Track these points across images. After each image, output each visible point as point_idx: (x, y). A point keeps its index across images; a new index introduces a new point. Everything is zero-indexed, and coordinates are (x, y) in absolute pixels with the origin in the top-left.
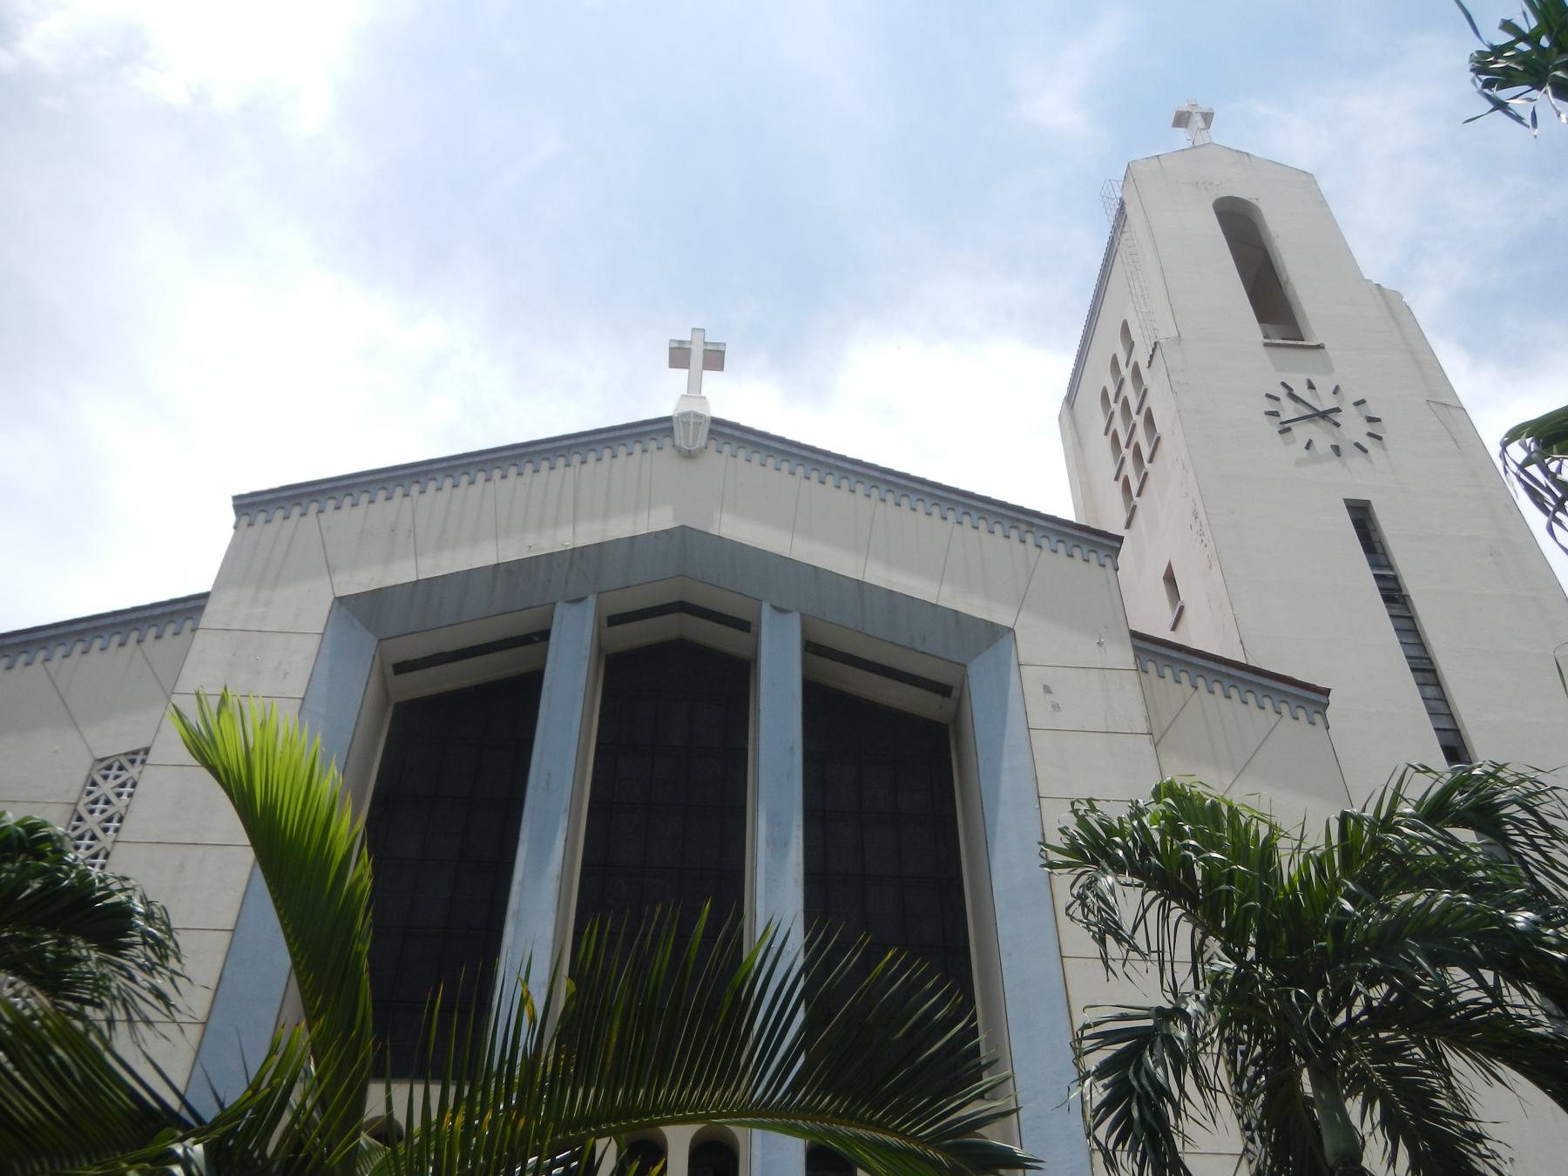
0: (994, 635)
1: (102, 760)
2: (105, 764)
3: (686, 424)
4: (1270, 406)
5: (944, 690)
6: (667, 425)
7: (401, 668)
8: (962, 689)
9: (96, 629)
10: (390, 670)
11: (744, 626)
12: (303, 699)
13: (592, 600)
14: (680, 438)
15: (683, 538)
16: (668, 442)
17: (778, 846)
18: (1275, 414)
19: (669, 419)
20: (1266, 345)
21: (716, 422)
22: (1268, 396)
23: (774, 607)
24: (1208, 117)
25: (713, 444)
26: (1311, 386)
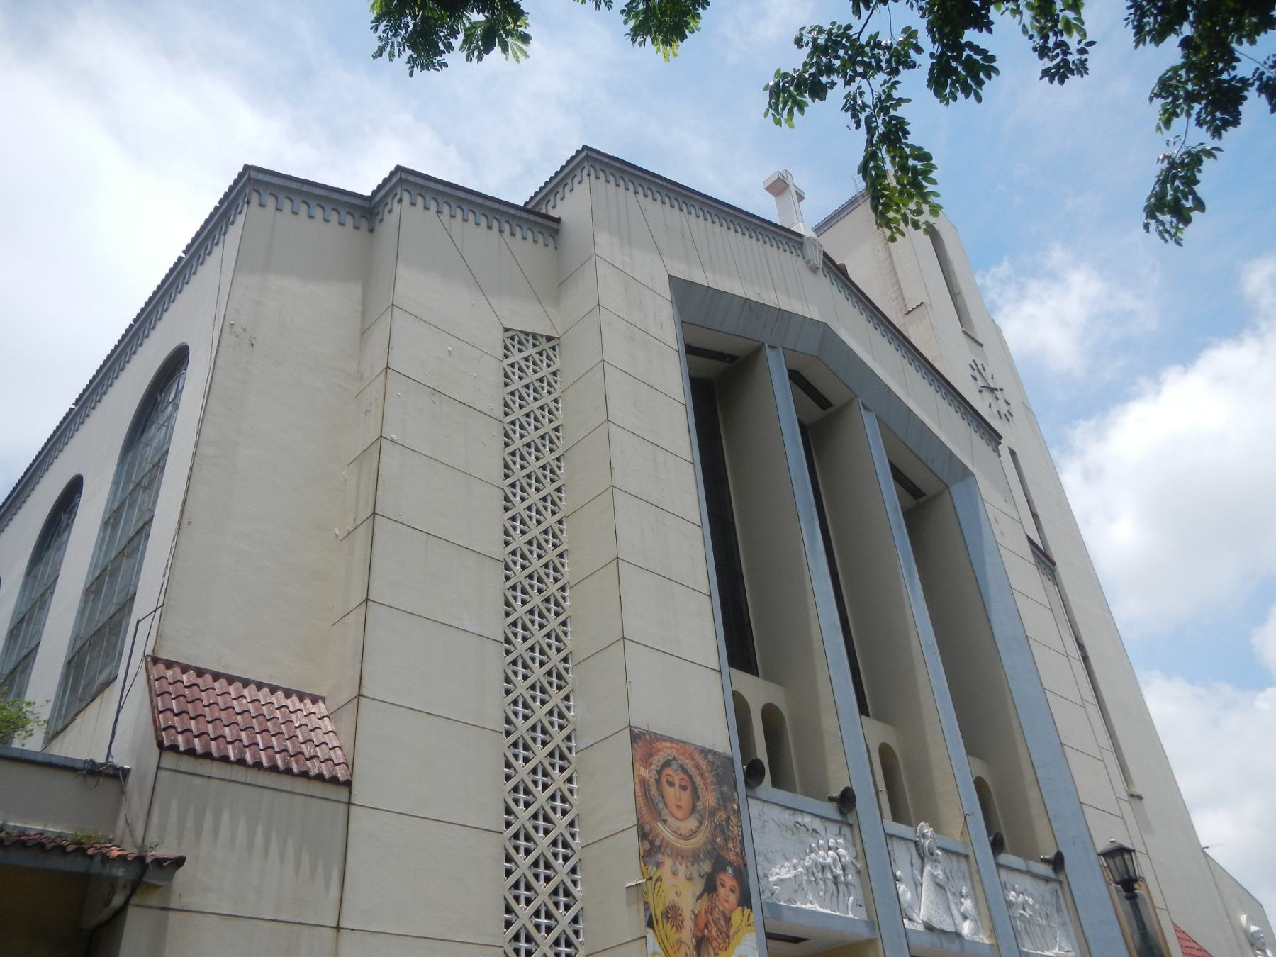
0: (966, 473)
1: (507, 330)
2: (510, 334)
4: (970, 372)
8: (936, 497)
9: (470, 202)
15: (824, 332)
17: (910, 573)
18: (975, 378)
19: (801, 236)
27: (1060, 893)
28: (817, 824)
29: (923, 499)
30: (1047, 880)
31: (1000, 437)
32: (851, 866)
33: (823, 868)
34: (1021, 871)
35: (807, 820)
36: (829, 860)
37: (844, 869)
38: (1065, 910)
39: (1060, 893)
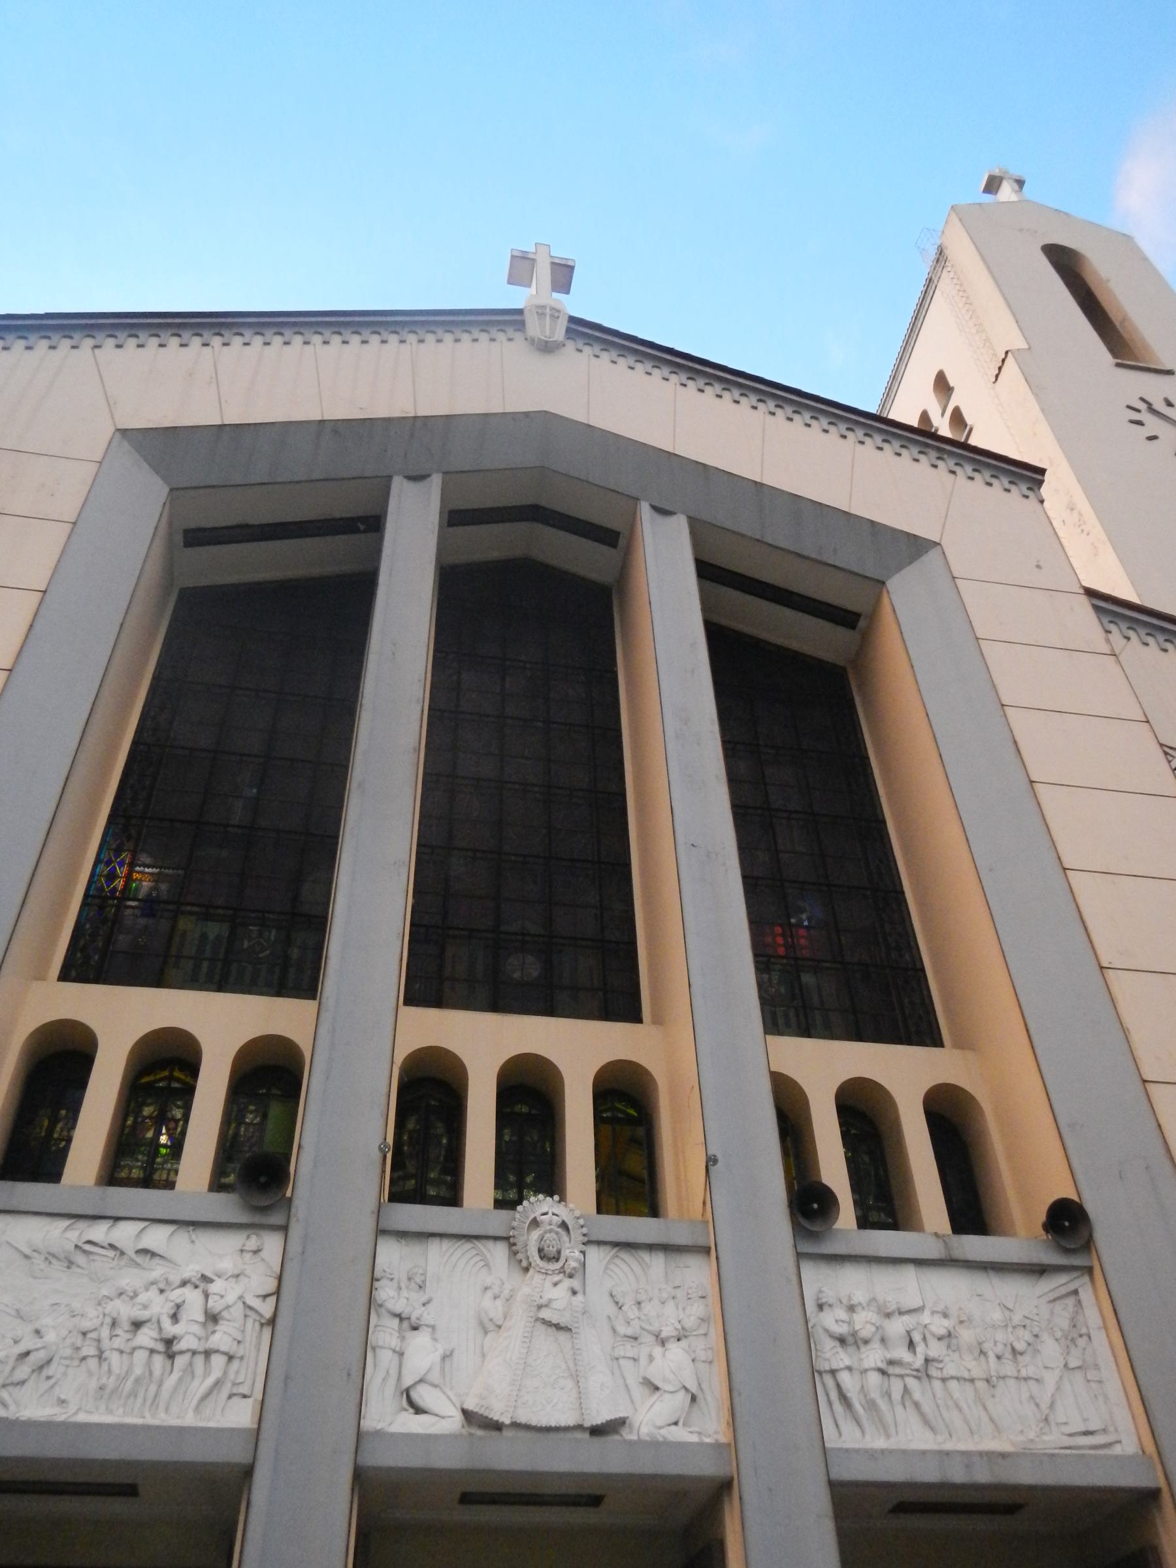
0: (916, 547)
3: (541, 315)
5: (846, 618)
6: (517, 317)
7: (196, 537)
10: (179, 539)
11: (608, 537)
12: (74, 523)
13: (436, 480)
14: (534, 328)
15: (544, 424)
16: (518, 336)
18: (1139, 423)
19: (520, 312)
20: (1118, 365)
21: (572, 319)
22: (1128, 407)
23: (656, 509)
24: (1020, 183)
25: (570, 345)
26: (1169, 404)
27: (1086, 1295)
28: (156, 1238)
29: (862, 623)
30: (1039, 1271)
31: (1042, 471)
32: (238, 1311)
33: (137, 1325)
34: (919, 1263)
35: (125, 1234)
36: (159, 1307)
37: (213, 1318)
38: (1099, 1338)
39: (1086, 1295)
